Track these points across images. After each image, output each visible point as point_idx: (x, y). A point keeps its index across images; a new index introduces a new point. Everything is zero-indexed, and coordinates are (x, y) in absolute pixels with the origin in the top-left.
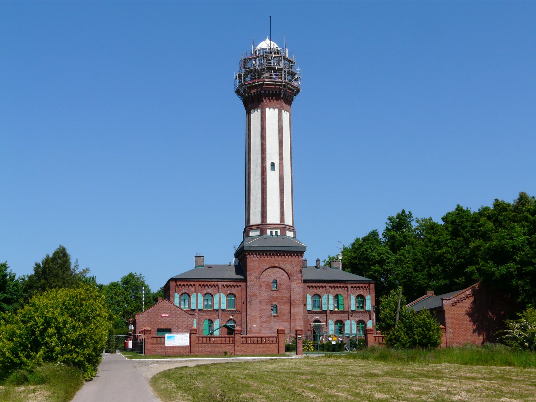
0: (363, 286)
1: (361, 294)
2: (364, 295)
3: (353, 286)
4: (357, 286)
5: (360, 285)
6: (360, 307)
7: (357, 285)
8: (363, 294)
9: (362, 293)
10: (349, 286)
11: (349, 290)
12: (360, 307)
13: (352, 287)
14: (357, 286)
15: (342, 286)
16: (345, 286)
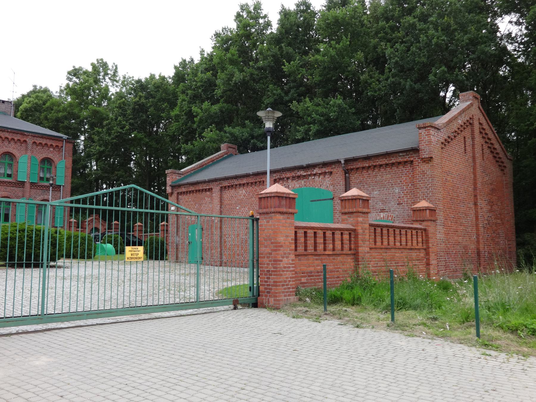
0: (54, 145)
1: (49, 156)
2: (55, 159)
3: (36, 141)
4: (44, 143)
5: (49, 142)
6: (45, 179)
7: (44, 141)
8: (52, 158)
9: (50, 156)
10: (30, 141)
11: (30, 146)
12: (45, 179)
13: (34, 143)
14: (44, 143)
15: (16, 139)
16: (22, 140)
